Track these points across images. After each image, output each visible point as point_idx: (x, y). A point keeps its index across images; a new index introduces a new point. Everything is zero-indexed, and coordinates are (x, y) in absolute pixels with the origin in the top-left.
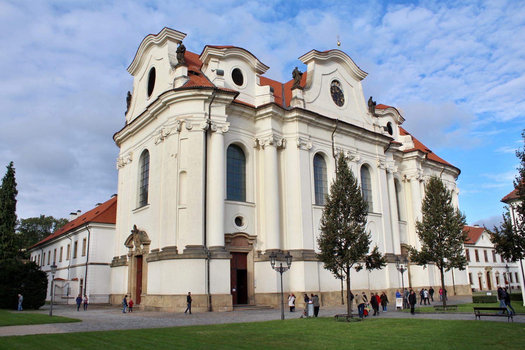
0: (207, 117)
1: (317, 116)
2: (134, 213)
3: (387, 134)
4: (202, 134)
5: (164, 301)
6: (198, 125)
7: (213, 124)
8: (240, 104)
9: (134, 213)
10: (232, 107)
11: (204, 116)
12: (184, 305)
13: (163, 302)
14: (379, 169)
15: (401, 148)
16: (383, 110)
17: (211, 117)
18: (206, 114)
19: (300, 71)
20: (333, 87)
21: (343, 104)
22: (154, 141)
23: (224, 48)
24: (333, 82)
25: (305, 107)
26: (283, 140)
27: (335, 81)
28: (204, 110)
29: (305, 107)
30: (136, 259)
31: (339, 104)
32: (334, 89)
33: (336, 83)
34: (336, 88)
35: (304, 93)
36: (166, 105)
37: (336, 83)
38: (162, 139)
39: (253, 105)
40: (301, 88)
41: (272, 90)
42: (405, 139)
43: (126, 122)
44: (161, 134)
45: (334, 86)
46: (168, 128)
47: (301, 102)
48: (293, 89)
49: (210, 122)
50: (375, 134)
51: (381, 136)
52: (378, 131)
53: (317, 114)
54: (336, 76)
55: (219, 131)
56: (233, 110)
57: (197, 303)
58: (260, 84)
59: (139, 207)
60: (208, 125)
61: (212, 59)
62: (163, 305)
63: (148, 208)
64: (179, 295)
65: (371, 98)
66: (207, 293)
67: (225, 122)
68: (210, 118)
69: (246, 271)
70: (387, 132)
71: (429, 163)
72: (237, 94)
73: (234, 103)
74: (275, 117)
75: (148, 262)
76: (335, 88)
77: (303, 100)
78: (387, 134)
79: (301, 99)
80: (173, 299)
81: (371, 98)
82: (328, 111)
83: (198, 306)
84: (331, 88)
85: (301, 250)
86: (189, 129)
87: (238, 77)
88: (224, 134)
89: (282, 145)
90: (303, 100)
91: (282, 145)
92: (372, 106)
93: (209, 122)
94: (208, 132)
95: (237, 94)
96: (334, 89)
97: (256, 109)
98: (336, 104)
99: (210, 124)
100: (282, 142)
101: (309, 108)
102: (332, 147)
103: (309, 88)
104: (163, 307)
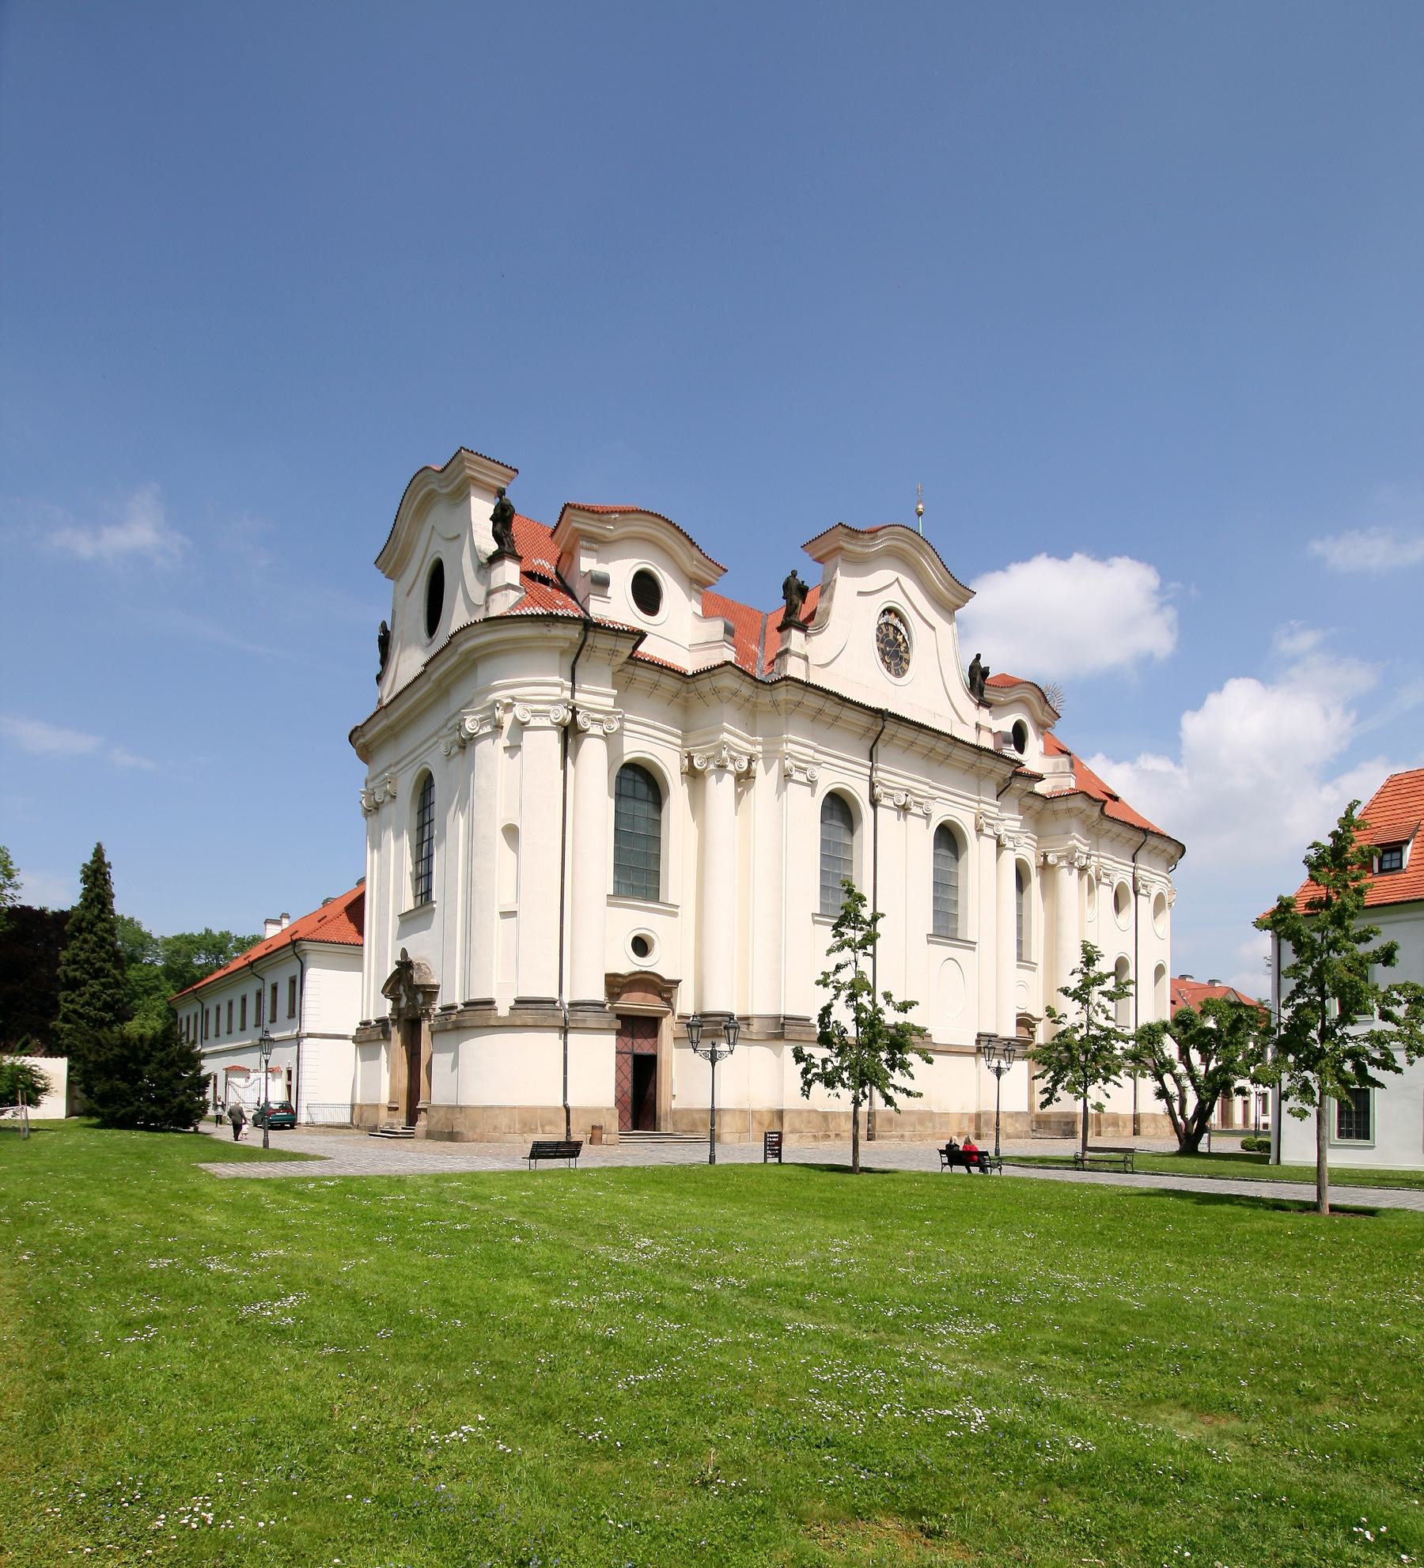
1: (837, 699)
3: (1010, 751)
4: (554, 739)
7: (581, 711)
8: (648, 662)
10: (631, 669)
15: (1040, 788)
16: (1007, 690)
19: (803, 582)
20: (883, 626)
21: (904, 672)
22: (442, 749)
23: (612, 512)
24: (884, 612)
25: (808, 676)
27: (889, 611)
29: (808, 676)
31: (895, 670)
32: (884, 630)
33: (893, 615)
34: (891, 629)
36: (470, 664)
37: (893, 615)
39: (681, 668)
40: (803, 627)
41: (729, 631)
42: (1056, 765)
43: (380, 701)
44: (457, 733)
45: (887, 624)
49: (574, 708)
50: (979, 750)
51: (997, 755)
52: (987, 742)
53: (836, 695)
54: (894, 598)
56: (631, 680)
58: (700, 614)
67: (611, 709)
68: (573, 697)
70: (1013, 747)
71: (1107, 825)
72: (641, 636)
73: (634, 659)
74: (734, 698)
76: (887, 630)
77: (806, 658)
78: (1010, 751)
79: (799, 656)
81: (978, 656)
82: (867, 687)
84: (879, 629)
86: (524, 724)
87: (647, 593)
88: (606, 736)
89: (749, 770)
90: (806, 658)
91: (749, 770)
92: (978, 679)
93: (571, 707)
95: (641, 636)
96: (884, 630)
97: (689, 677)
98: (889, 669)
99: (574, 712)
101: (817, 679)
102: (868, 778)
103: (821, 628)
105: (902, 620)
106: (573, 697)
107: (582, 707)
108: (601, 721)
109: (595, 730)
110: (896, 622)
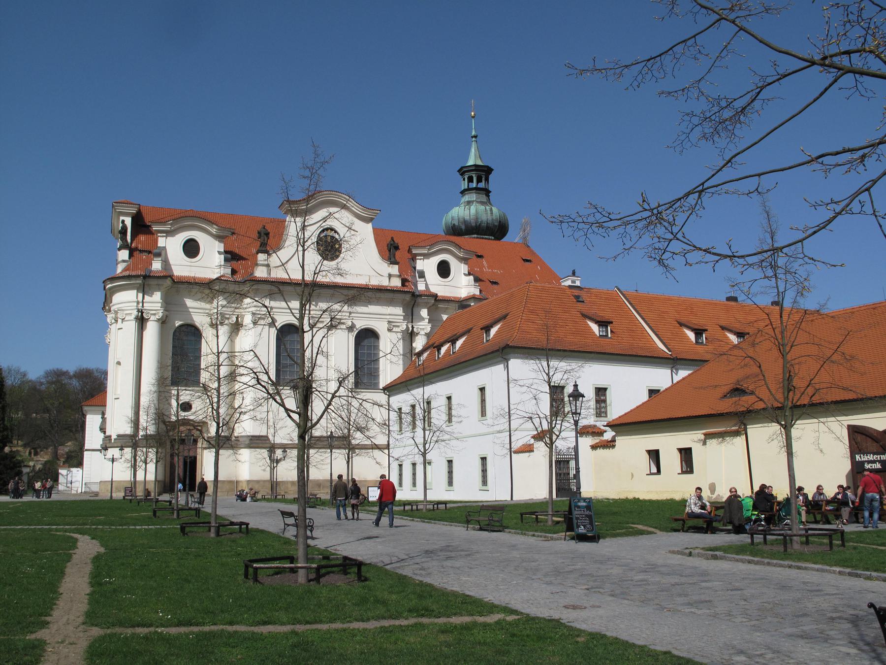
0: (141, 305)
6: (131, 314)
11: (135, 304)
14: (389, 334)
17: (145, 305)
18: (138, 303)
24: (323, 231)
26: (238, 316)
27: (327, 229)
28: (137, 298)
34: (329, 238)
35: (269, 255)
40: (266, 252)
45: (326, 236)
47: (265, 269)
48: (257, 253)
54: (330, 223)
55: (152, 318)
60: (140, 314)
61: (159, 235)
65: (392, 238)
66: (132, 479)
67: (159, 308)
68: (143, 306)
69: (195, 458)
85: (249, 436)
90: (268, 266)
94: (142, 321)
99: (142, 313)
100: (237, 318)
105: (336, 232)
106: (143, 306)
107: (145, 310)
108: (154, 314)
109: (152, 318)
110: (332, 234)
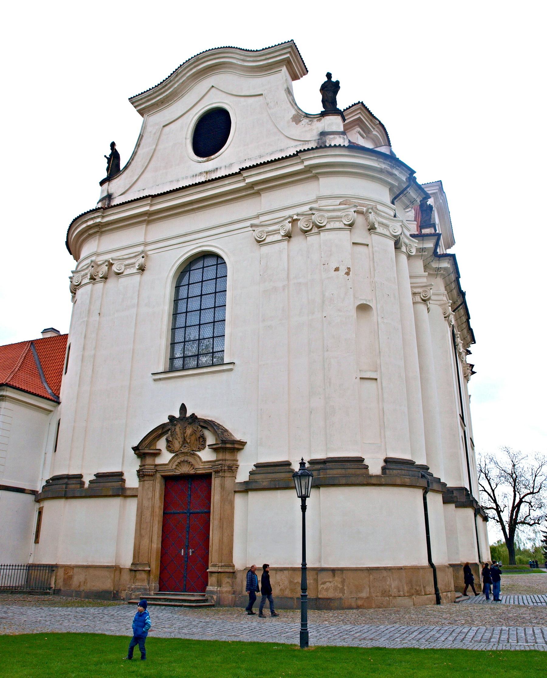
2: (155, 380)
5: (343, 582)
9: (155, 380)
12: (399, 592)
13: (340, 586)
30: (163, 482)
38: (289, 236)
46: (323, 216)
57: (422, 586)
59: (161, 369)
62: (342, 591)
63: (231, 370)
64: (385, 569)
75: (235, 492)
80: (371, 576)
83: (423, 594)
104: (341, 599)
